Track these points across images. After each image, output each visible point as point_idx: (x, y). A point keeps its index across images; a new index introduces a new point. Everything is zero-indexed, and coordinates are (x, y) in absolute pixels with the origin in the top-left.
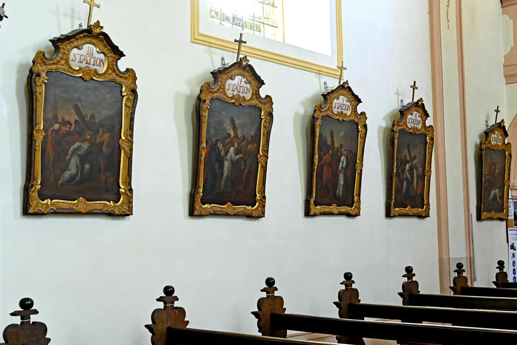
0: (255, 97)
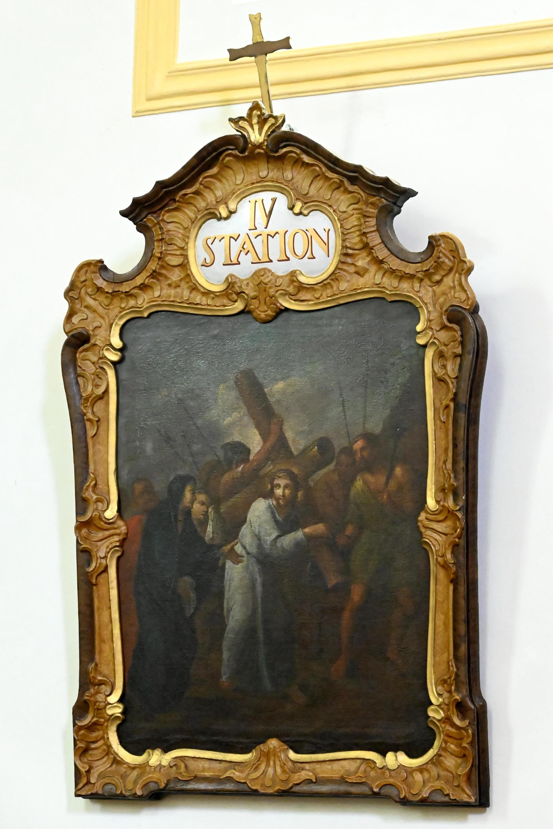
0: (368, 259)
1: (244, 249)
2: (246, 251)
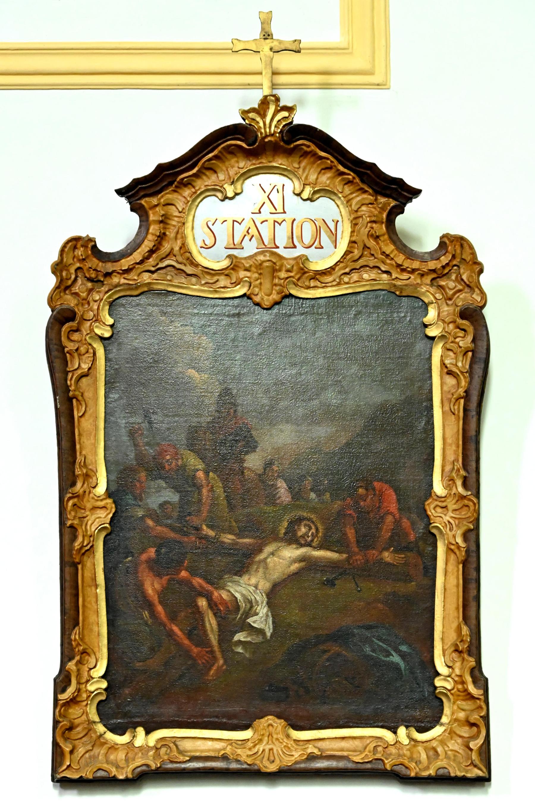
1: (249, 233)
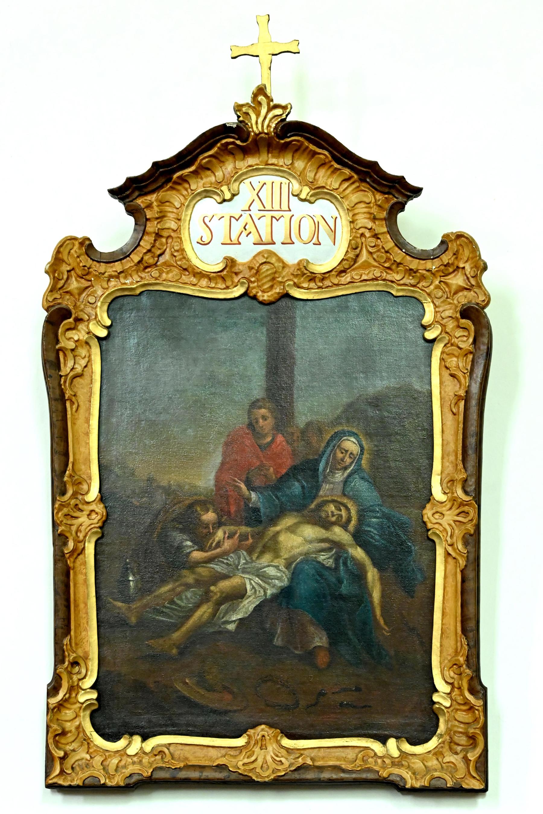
1: (246, 230)
2: (248, 232)
